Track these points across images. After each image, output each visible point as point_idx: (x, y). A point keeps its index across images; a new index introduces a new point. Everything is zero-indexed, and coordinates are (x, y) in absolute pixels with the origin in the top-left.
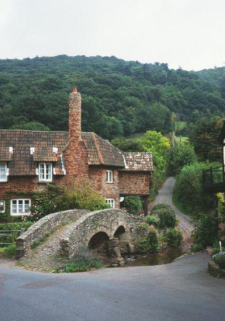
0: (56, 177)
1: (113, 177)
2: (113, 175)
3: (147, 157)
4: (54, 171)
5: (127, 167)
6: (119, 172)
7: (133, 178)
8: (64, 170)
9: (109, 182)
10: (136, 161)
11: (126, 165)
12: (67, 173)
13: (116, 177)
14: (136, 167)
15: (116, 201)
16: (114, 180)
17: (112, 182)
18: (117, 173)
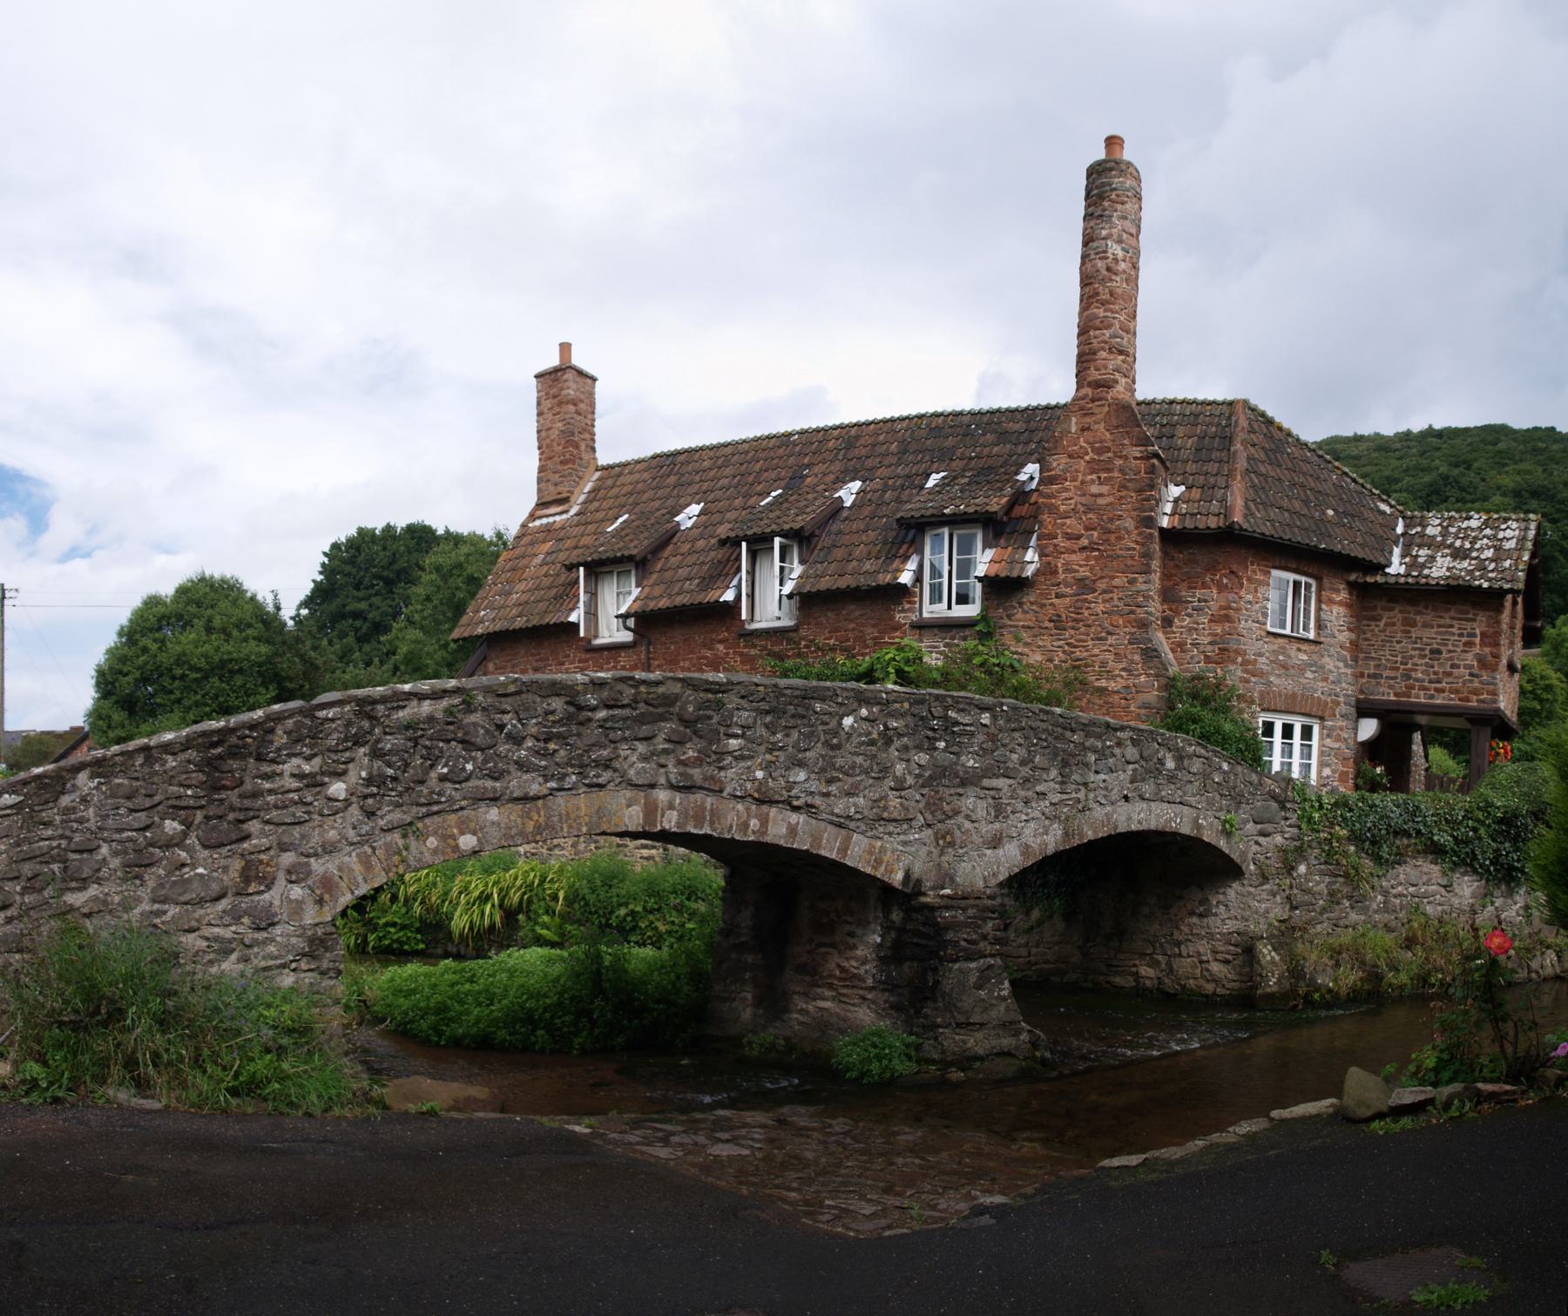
0: (1001, 588)
1: (1319, 609)
2: (1319, 601)
3: (1509, 533)
4: (984, 561)
5: (1396, 567)
6: (1352, 586)
7: (1425, 625)
8: (1030, 555)
9: (1288, 631)
10: (1449, 547)
11: (1396, 559)
12: (1047, 570)
13: (1337, 615)
14: (1441, 569)
15: (1327, 733)
16: (1320, 626)
17: (1312, 635)
18: (1343, 595)
